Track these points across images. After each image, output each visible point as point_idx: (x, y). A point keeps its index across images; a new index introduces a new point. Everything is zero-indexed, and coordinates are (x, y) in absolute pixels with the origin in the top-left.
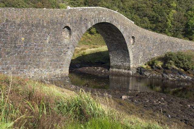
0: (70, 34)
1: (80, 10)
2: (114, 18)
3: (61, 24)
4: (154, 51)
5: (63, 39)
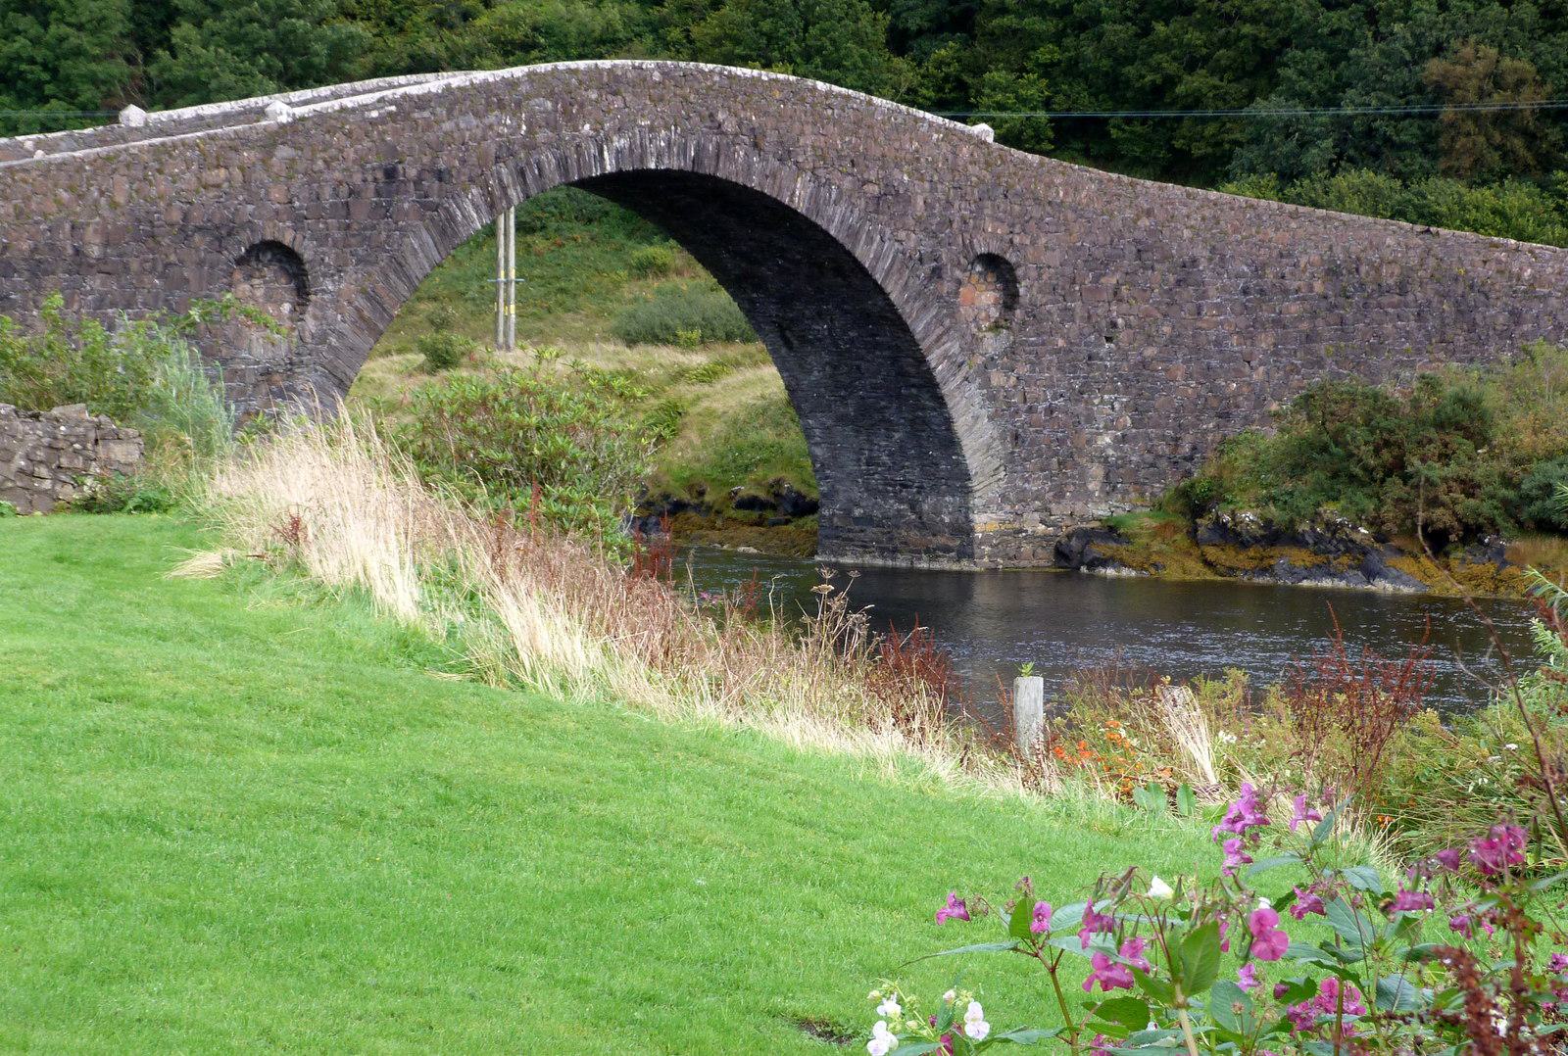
0: (302, 292)
1: (375, 114)
2: (730, 126)
3: (221, 233)
4: (1258, 375)
5: (239, 333)
